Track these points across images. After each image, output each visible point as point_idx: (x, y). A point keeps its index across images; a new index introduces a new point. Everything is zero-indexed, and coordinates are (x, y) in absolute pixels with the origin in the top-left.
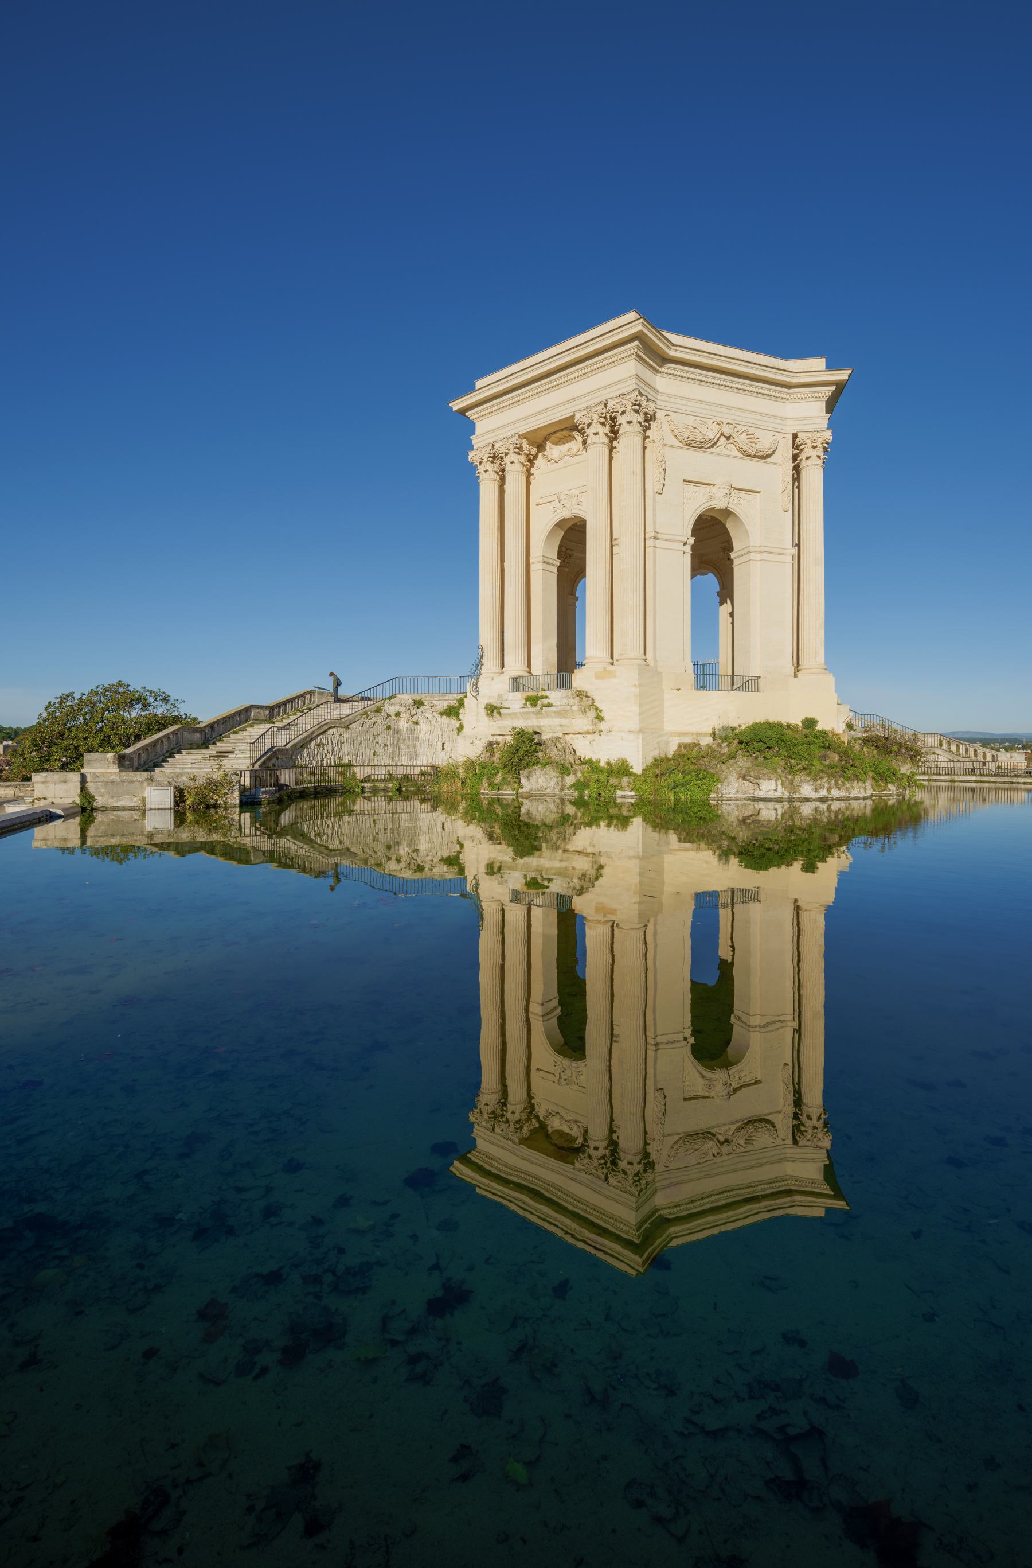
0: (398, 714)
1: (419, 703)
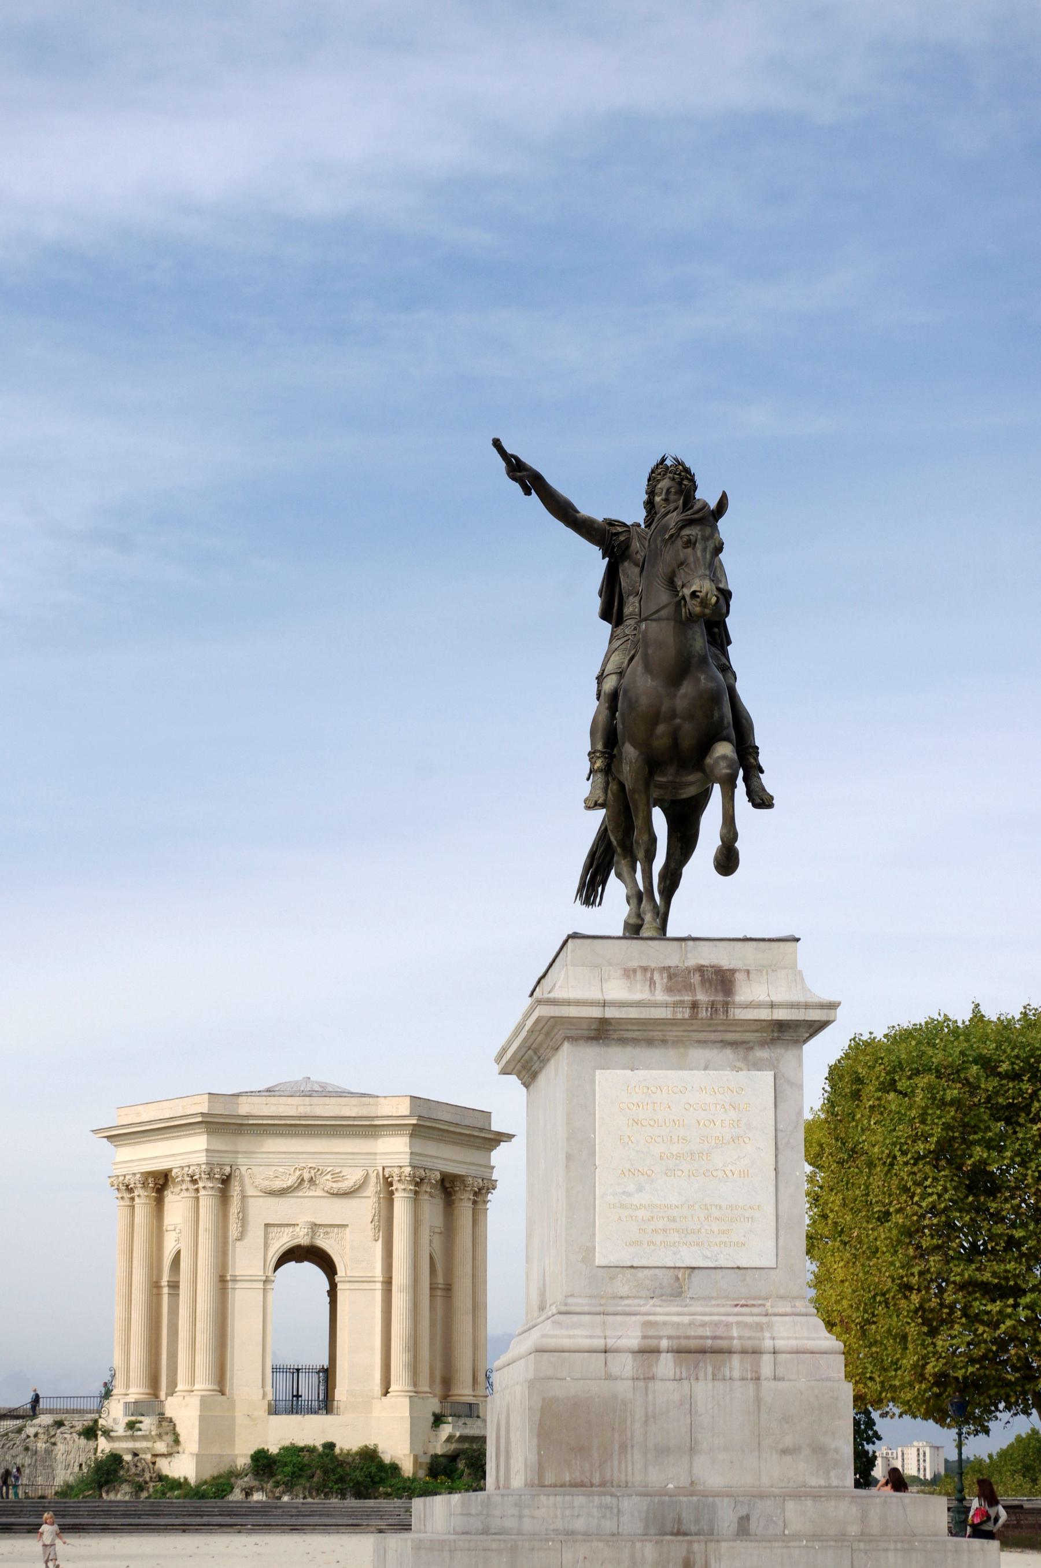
0: (36, 1435)
1: (60, 1424)
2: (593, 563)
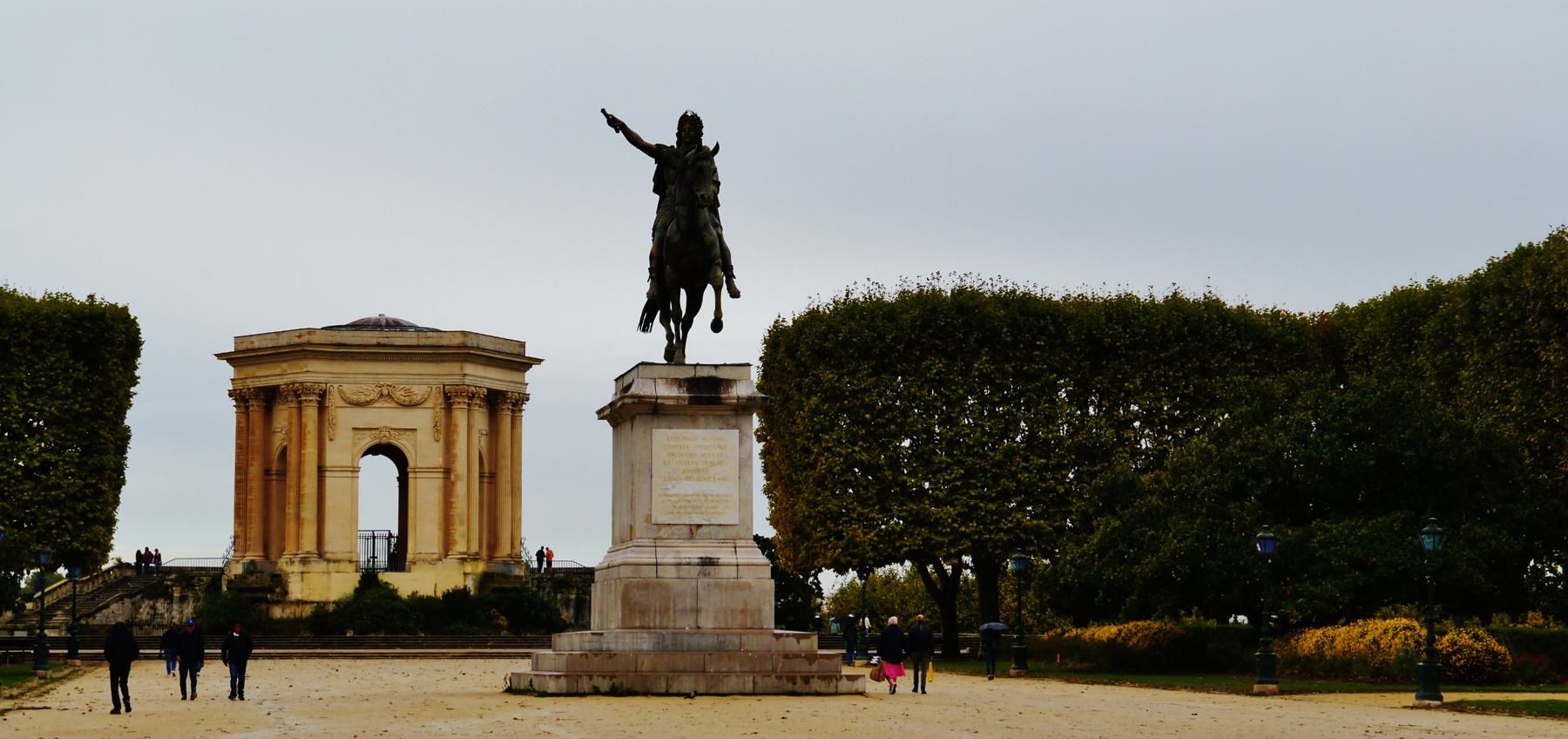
2: (650, 165)
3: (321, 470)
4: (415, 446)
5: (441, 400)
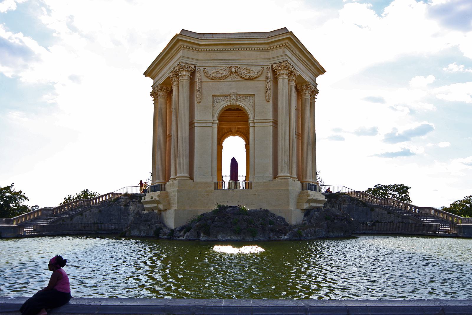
3: (192, 124)
4: (254, 106)
5: (270, 74)
